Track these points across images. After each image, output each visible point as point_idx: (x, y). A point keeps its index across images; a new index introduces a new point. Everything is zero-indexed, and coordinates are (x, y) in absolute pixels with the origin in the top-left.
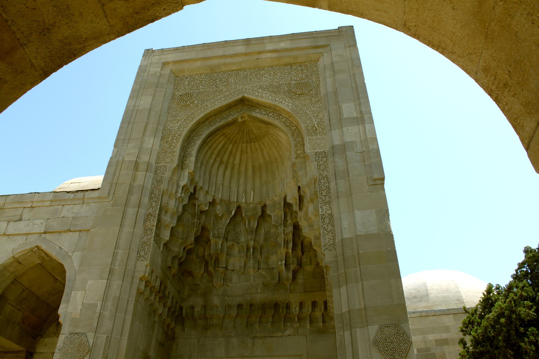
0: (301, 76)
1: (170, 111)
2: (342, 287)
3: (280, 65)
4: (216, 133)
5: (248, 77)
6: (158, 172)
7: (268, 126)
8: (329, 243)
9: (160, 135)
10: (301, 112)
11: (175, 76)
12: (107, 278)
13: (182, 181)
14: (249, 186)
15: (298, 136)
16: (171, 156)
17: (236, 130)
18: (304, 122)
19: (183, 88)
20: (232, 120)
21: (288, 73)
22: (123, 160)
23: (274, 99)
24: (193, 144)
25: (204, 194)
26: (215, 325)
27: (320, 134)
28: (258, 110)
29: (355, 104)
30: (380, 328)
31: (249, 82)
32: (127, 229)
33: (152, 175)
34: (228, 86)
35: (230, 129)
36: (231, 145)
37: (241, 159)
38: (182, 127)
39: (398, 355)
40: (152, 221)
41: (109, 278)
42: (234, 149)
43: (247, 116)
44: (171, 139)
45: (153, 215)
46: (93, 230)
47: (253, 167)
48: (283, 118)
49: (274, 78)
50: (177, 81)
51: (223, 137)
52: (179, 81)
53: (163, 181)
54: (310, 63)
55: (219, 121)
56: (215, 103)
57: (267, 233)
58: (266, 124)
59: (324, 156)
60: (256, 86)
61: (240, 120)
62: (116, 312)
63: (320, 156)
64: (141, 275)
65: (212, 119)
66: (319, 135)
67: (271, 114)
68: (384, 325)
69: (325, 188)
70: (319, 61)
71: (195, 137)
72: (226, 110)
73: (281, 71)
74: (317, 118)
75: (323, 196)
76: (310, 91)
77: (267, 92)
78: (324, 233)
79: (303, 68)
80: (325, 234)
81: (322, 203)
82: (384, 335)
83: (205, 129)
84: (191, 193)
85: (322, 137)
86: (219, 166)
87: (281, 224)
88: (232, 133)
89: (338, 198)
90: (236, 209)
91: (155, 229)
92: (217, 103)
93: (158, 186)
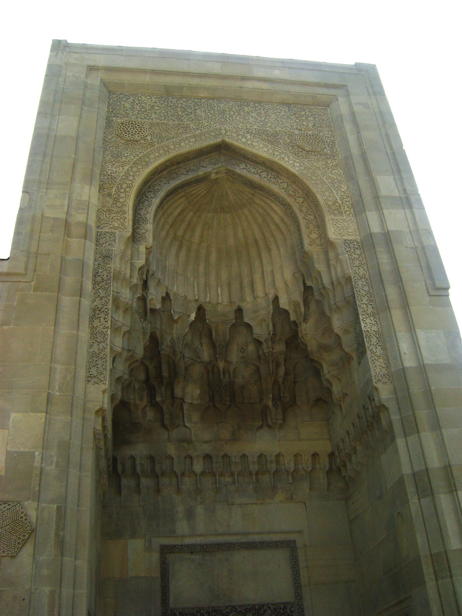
4: (178, 191)
6: (102, 241)
7: (257, 191)
8: (381, 373)
9: (96, 183)
11: (108, 91)
12: (45, 410)
13: (138, 260)
15: (308, 213)
17: (204, 191)
19: (123, 112)
24: (146, 203)
27: (346, 214)
28: (243, 166)
29: (395, 178)
31: (229, 121)
32: (64, 330)
33: (93, 245)
34: (198, 122)
36: (191, 213)
37: (202, 236)
38: (132, 174)
40: (102, 319)
43: (224, 172)
44: (115, 191)
48: (283, 182)
50: (112, 100)
52: (115, 99)
56: (180, 144)
57: (242, 350)
59: (356, 247)
60: (240, 128)
61: (213, 176)
62: (68, 467)
64: (98, 408)
65: (173, 168)
66: (345, 216)
67: (264, 174)
69: (365, 293)
71: (149, 193)
72: (195, 158)
73: (275, 111)
74: (339, 190)
76: (324, 149)
78: (372, 358)
79: (307, 113)
83: (163, 182)
85: (349, 218)
89: (389, 310)
91: (109, 334)
92: (183, 144)
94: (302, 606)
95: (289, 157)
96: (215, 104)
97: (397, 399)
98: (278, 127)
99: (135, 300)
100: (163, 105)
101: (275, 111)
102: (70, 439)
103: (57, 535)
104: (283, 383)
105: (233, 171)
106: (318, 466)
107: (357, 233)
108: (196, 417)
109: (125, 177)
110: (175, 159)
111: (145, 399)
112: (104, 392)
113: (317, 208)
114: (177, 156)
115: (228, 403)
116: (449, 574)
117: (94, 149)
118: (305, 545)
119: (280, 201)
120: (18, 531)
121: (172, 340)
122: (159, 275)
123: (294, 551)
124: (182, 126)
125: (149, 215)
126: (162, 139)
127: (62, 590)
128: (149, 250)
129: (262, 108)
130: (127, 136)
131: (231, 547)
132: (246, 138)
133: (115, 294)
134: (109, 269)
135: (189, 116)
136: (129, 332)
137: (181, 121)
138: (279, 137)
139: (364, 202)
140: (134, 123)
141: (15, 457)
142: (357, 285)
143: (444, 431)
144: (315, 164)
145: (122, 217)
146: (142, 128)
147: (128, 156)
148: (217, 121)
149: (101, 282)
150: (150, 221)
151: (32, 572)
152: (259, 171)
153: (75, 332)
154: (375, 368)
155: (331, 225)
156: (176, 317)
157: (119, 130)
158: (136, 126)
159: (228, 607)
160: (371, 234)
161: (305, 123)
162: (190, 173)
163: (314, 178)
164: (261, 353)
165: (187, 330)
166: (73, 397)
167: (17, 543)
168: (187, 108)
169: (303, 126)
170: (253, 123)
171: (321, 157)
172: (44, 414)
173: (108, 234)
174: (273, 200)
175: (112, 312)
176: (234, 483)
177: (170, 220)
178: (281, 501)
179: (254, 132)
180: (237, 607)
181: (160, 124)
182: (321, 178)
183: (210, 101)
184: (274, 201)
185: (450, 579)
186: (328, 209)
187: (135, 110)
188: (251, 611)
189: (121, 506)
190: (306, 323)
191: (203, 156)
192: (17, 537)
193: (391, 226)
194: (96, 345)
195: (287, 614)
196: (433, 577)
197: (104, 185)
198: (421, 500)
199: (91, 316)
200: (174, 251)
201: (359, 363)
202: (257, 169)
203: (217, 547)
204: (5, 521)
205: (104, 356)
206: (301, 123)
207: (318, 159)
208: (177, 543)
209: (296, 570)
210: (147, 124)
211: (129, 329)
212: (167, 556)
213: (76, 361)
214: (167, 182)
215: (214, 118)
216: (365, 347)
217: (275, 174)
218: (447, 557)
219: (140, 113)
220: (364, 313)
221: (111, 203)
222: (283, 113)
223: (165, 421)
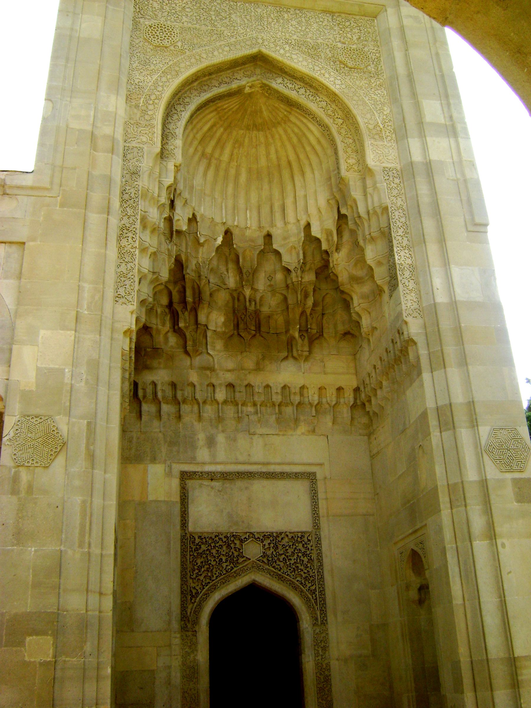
2: (435, 371)
3: (316, 10)
5: (264, 19)
6: (129, 157)
7: (293, 108)
8: (412, 307)
9: (123, 92)
12: (74, 328)
14: (241, 202)
15: (347, 136)
16: (147, 132)
18: (363, 115)
19: (151, 13)
20: (238, 88)
21: (329, 27)
24: (175, 117)
27: (388, 140)
28: (280, 80)
30: (494, 430)
31: (266, 29)
32: (92, 248)
34: (232, 28)
35: (229, 101)
38: (161, 84)
39: (516, 465)
40: (130, 239)
41: (78, 329)
42: (225, 136)
43: (259, 86)
44: (143, 102)
45: (130, 229)
46: (32, 244)
47: (250, 170)
48: (322, 101)
49: (307, 30)
51: (214, 113)
54: (363, 18)
55: (217, 85)
56: (213, 53)
58: (291, 105)
59: (396, 175)
61: (247, 90)
62: (97, 385)
63: (390, 173)
64: (126, 328)
65: (205, 79)
66: (385, 141)
67: (302, 91)
68: (499, 427)
70: (378, 17)
71: (179, 106)
72: (229, 69)
73: (317, 20)
74: (381, 113)
76: (368, 66)
77: (299, 53)
82: (499, 440)
85: (390, 144)
86: (200, 160)
88: (229, 108)
89: (425, 242)
92: (216, 53)
94: (320, 535)
96: (252, 9)
97: (426, 333)
98: (320, 39)
99: (163, 220)
100: (195, 7)
101: (317, 20)
102: (99, 358)
103: (87, 448)
104: (311, 314)
105: (268, 86)
106: (342, 400)
107: (398, 161)
108: (219, 345)
109: (153, 88)
110: (207, 69)
111: (168, 325)
112: (132, 313)
113: (357, 132)
114: (210, 67)
115: (254, 332)
116: (464, 503)
117: (121, 54)
118: (325, 478)
119: (317, 121)
120: (51, 444)
121: (198, 265)
122: (186, 195)
123: (314, 482)
124: (216, 32)
125: (178, 130)
126: (193, 46)
127: (93, 500)
128: (177, 168)
129: (303, 16)
130: (156, 41)
132: (284, 49)
133: (143, 213)
134: (137, 186)
135: (224, 21)
136: (155, 254)
137: (215, 26)
138: (320, 49)
139: (408, 127)
140: (164, 27)
141: (45, 373)
143: (470, 367)
144: (358, 83)
145: (150, 131)
146: (172, 33)
147: (156, 63)
148: (253, 28)
149: (129, 200)
150: (179, 136)
151: (65, 482)
152: (297, 87)
153: (103, 251)
154: (406, 302)
155: (371, 152)
156: (202, 240)
157: (147, 33)
158: (166, 30)
159: (246, 533)
160: (412, 163)
161: (349, 36)
162: (222, 86)
163: (355, 98)
164: (289, 282)
165: (214, 254)
166: (101, 316)
167: (49, 454)
168: (221, 11)
169: (346, 39)
170: (293, 32)
171: (365, 75)
172: (74, 332)
173: (136, 150)
174: (310, 119)
175: (140, 232)
176: (256, 413)
177: (199, 136)
178: (303, 434)
179: (293, 43)
180: (255, 534)
181: (192, 29)
182: (363, 98)
183: (247, 5)
184: (311, 120)
185: (464, 508)
186: (368, 133)
187: (164, 11)
188: (269, 538)
189: (141, 432)
190: (338, 253)
191: (237, 67)
192: (50, 450)
193: (434, 156)
194: (123, 265)
196: (448, 505)
197: (131, 95)
198: (442, 433)
199: (119, 235)
200: (201, 169)
201: (391, 296)
203: (237, 475)
204: (38, 434)
205: (132, 277)
206: (345, 35)
207: (361, 77)
208: (197, 470)
210: (177, 28)
211: (155, 250)
212: (187, 481)
213: (104, 280)
214: (198, 95)
215: (250, 24)
216: (397, 280)
217: (314, 91)
218: (463, 487)
219: (170, 14)
220: (399, 246)
221: (138, 115)
222: (326, 23)
223: (188, 348)
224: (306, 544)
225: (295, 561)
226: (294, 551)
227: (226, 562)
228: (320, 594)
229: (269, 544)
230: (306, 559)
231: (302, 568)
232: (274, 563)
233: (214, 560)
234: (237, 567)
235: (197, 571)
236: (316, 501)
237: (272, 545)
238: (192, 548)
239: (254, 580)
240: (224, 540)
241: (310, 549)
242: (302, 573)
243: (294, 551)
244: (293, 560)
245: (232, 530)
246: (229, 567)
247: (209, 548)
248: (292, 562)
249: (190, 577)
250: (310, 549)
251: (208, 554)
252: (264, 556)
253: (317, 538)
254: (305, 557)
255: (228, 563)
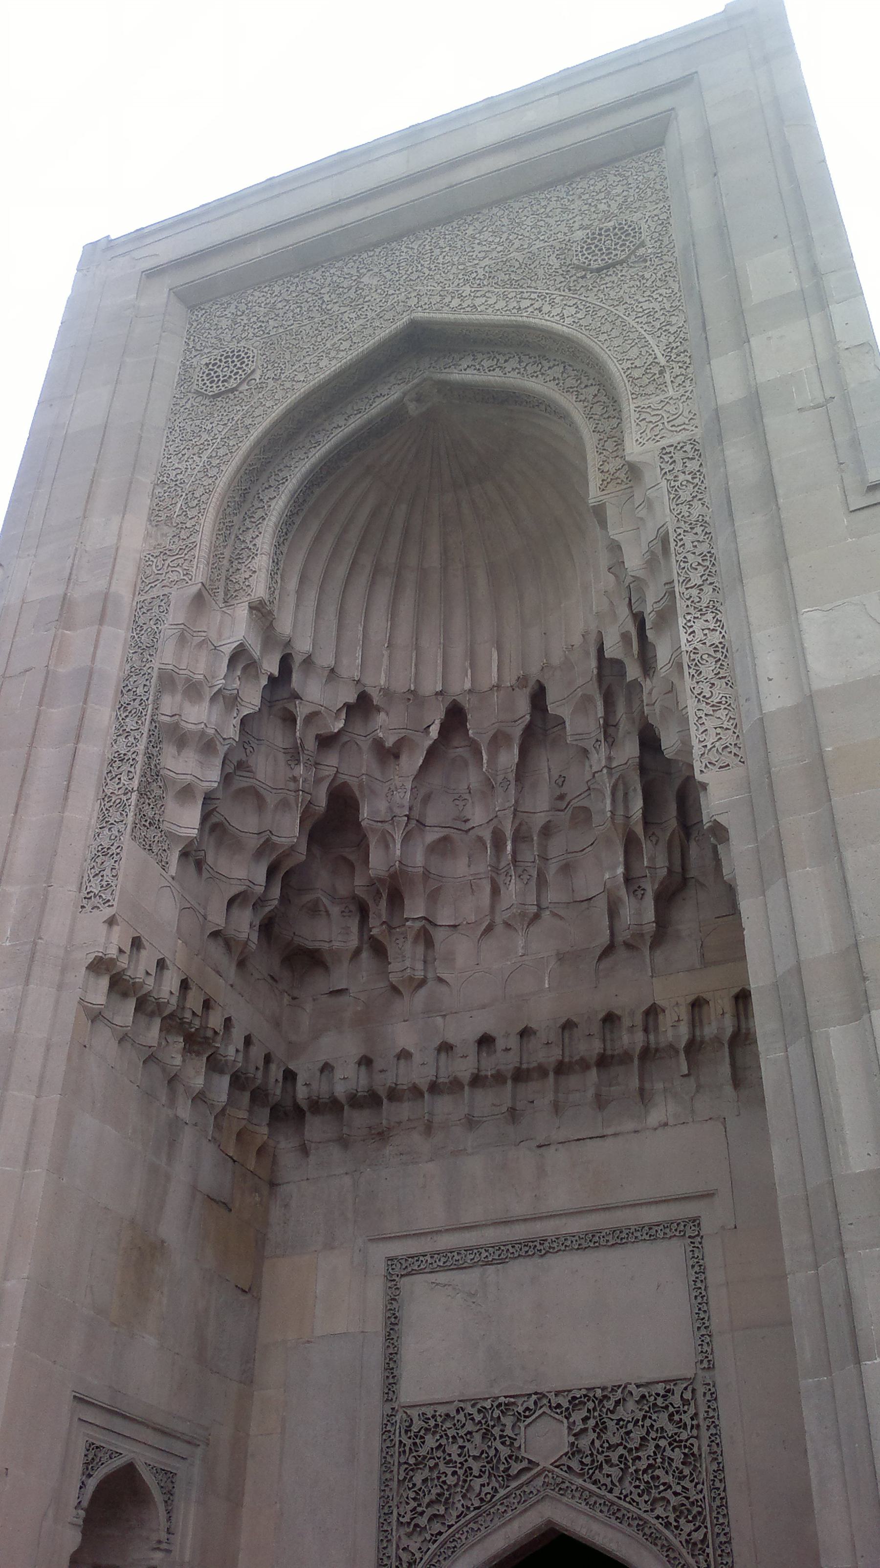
0: (606, 208)
1: (177, 423)
5: (425, 256)
10: (607, 327)
15: (606, 416)
19: (213, 340)
22: (23, 601)
23: (515, 304)
25: (324, 681)
26: (409, 1120)
31: (427, 272)
36: (404, 507)
53: (159, 645)
61: (412, 408)
63: (678, 456)
67: (513, 363)
75: (692, 587)
78: (700, 714)
80: (703, 716)
81: (688, 614)
84: (271, 678)
86: (373, 583)
87: (597, 741)
90: (443, 717)
93: (144, 664)
95: (552, 304)
109: (202, 474)
131: (544, 1249)
142: (680, 547)
144: (612, 294)
159: (530, 1395)
180: (552, 1396)
194: (106, 831)
195: (674, 1408)
202: (498, 357)
203: (511, 1250)
207: (623, 278)
209: (701, 1293)
224: (677, 1412)
225: (651, 1461)
226: (648, 1433)
227: (480, 1476)
228: (719, 1552)
229: (585, 1420)
230: (677, 1455)
231: (669, 1479)
232: (597, 1471)
233: (454, 1473)
234: (508, 1486)
235: (413, 1504)
236: (704, 1293)
237: (591, 1423)
238: (405, 1445)
239: (549, 1522)
240: (478, 1418)
241: (689, 1428)
242: (668, 1494)
243: (648, 1433)
244: (644, 1458)
245: (496, 1392)
246: (487, 1489)
247: (443, 1441)
248: (643, 1464)
249: (398, 1519)
250: (689, 1428)
251: (439, 1458)
252: (573, 1454)
253: (708, 1394)
254: (677, 1450)
255: (484, 1480)
